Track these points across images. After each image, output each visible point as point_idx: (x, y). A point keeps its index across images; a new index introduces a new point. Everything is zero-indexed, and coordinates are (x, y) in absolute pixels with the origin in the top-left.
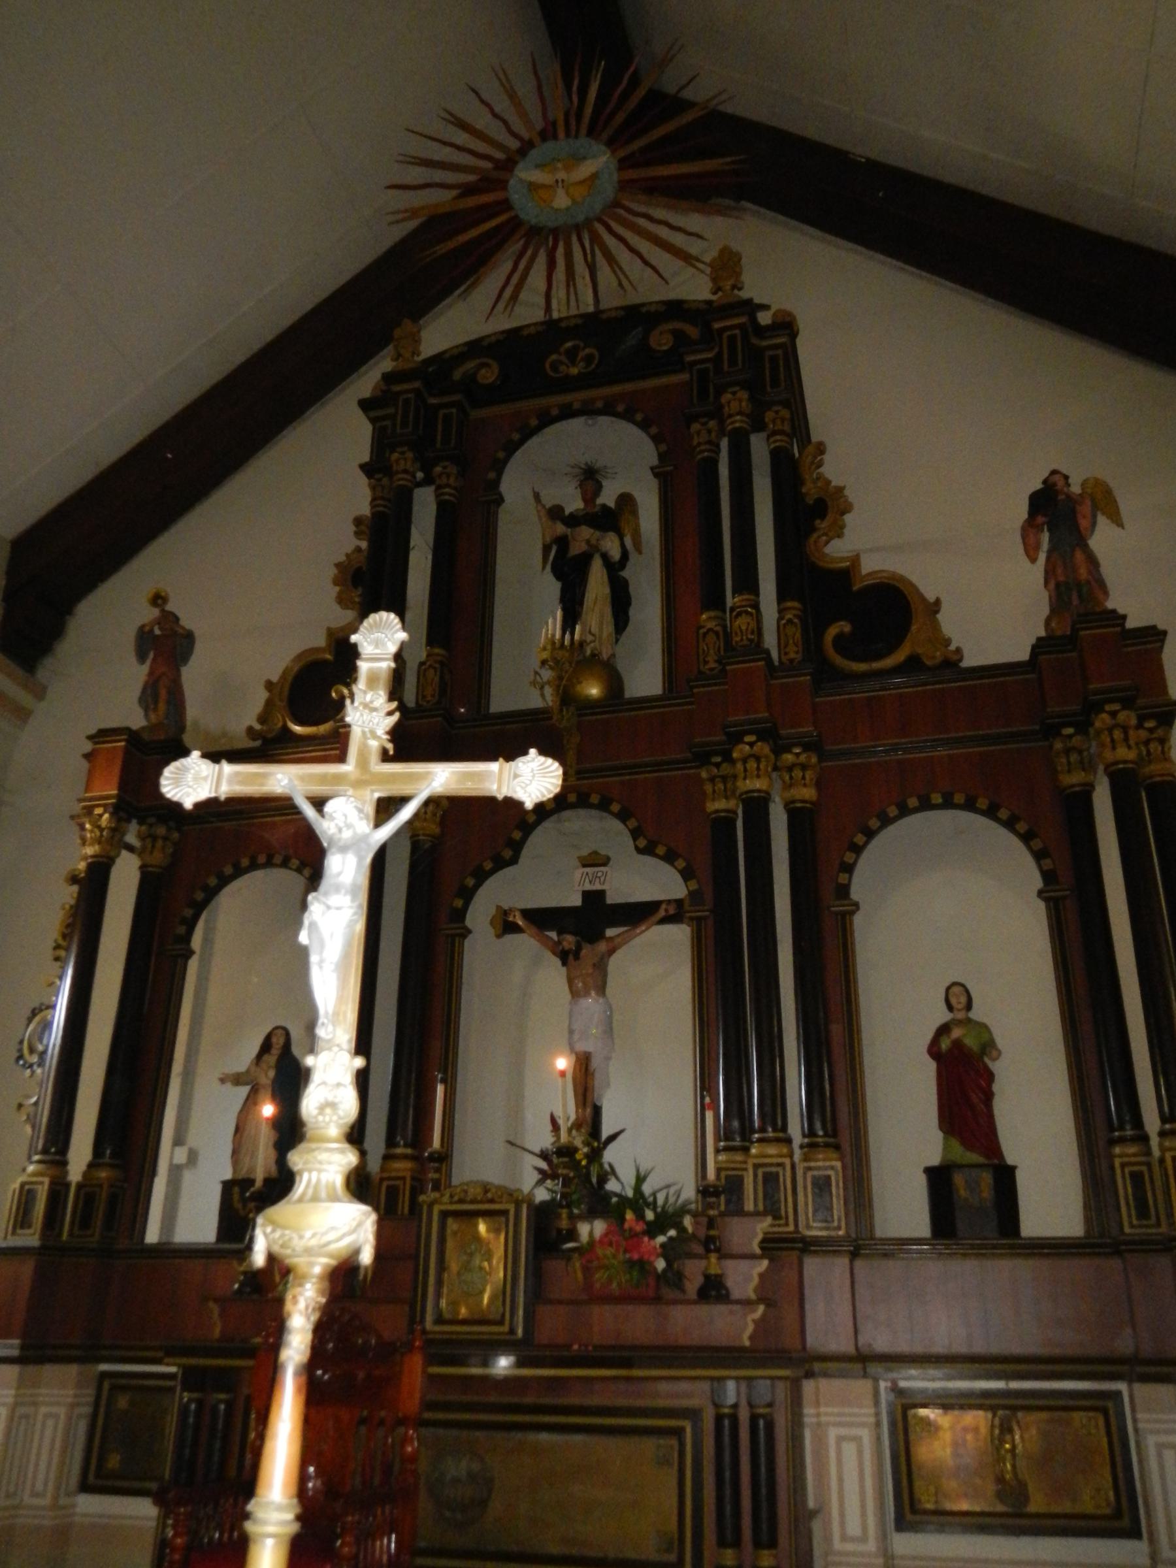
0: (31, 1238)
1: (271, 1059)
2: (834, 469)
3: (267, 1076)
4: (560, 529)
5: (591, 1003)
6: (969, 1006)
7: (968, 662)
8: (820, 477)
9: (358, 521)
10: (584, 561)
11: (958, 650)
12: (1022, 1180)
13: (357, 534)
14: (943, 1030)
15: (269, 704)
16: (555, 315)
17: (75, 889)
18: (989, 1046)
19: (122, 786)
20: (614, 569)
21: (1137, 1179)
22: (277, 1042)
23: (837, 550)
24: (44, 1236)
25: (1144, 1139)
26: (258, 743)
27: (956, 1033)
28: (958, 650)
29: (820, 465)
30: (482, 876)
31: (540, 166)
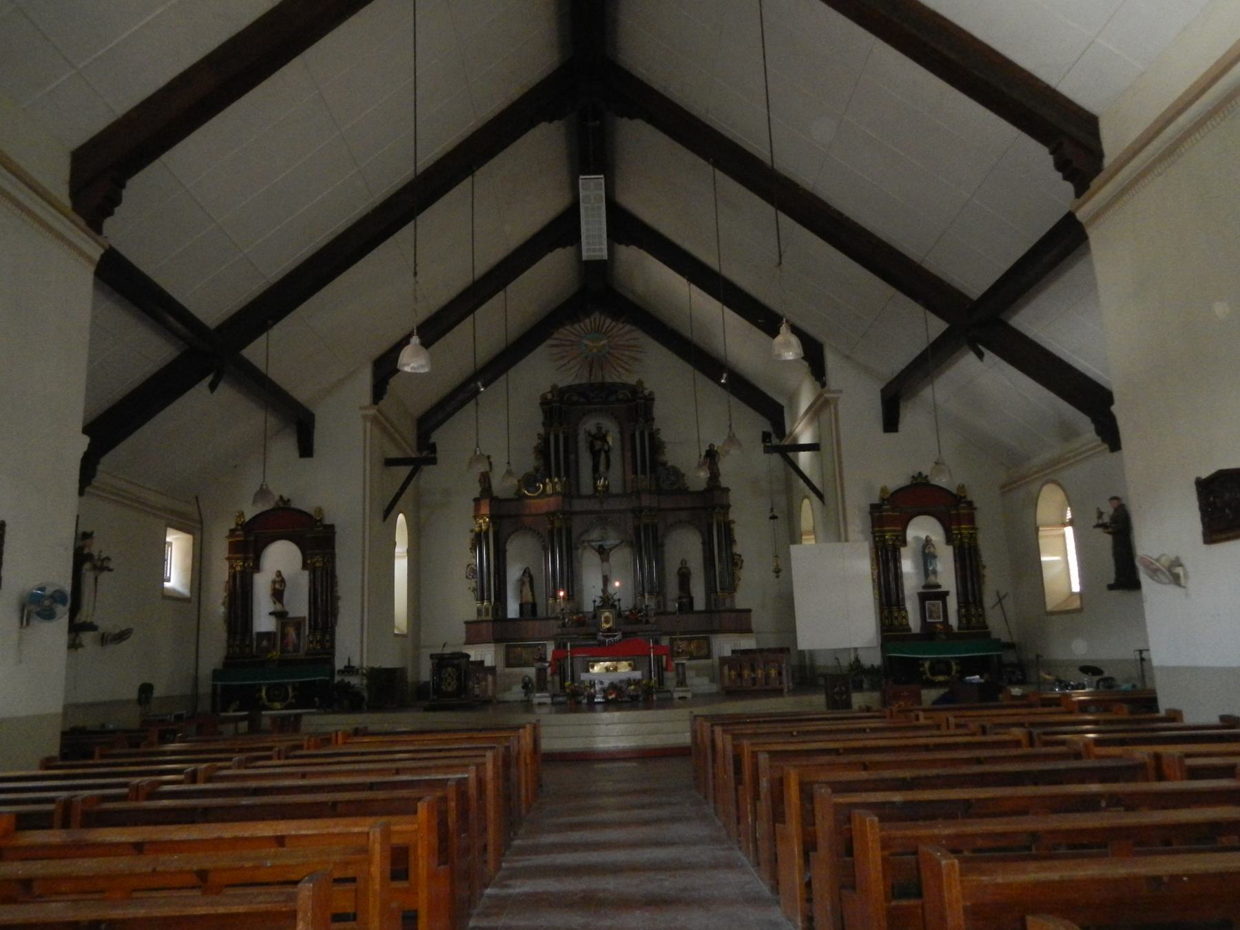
0: (490, 617)
1: (527, 575)
2: (664, 436)
3: (527, 580)
4: (591, 439)
5: (605, 563)
6: (686, 564)
7: (691, 489)
8: (659, 438)
9: (539, 435)
10: (599, 451)
11: (688, 487)
12: (695, 600)
13: (539, 438)
14: (680, 569)
15: (519, 486)
16: (592, 381)
17: (473, 534)
18: (689, 573)
19: (490, 510)
20: (607, 452)
21: (716, 600)
22: (527, 570)
23: (664, 458)
24: (493, 617)
25: (717, 592)
26: (517, 497)
27: (684, 570)
28: (688, 487)
29: (659, 433)
30: (581, 534)
31: (588, 339)
